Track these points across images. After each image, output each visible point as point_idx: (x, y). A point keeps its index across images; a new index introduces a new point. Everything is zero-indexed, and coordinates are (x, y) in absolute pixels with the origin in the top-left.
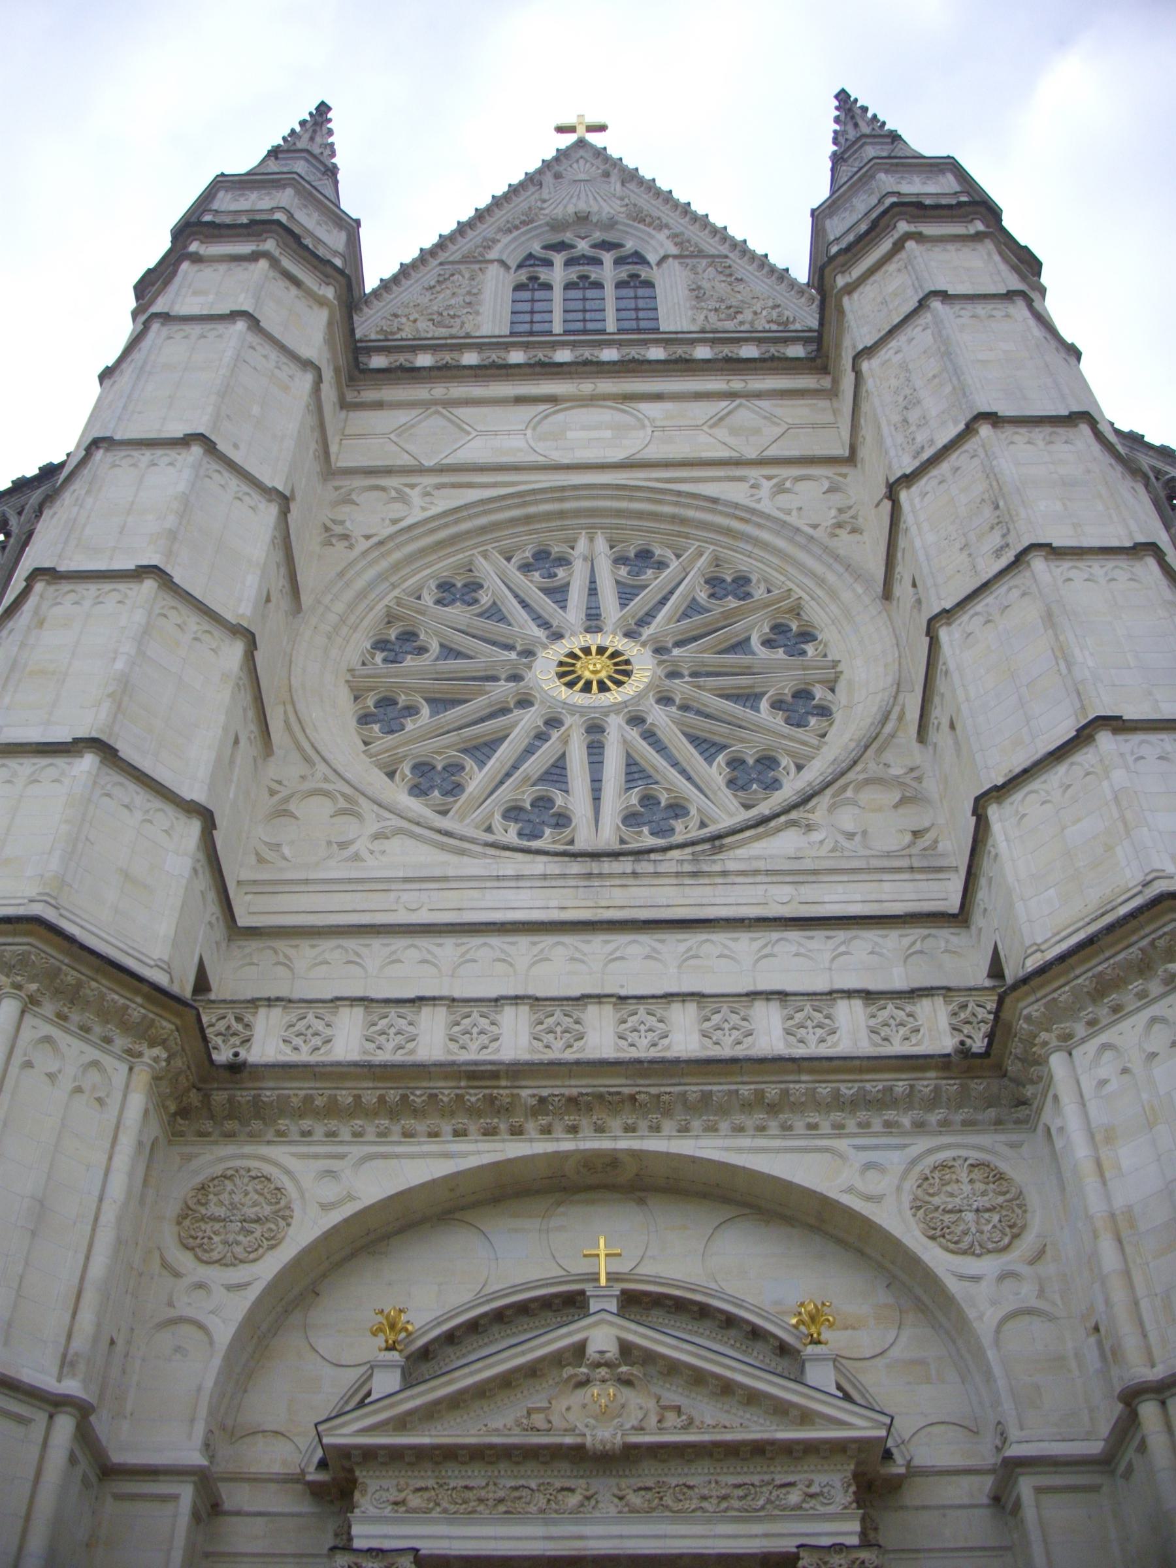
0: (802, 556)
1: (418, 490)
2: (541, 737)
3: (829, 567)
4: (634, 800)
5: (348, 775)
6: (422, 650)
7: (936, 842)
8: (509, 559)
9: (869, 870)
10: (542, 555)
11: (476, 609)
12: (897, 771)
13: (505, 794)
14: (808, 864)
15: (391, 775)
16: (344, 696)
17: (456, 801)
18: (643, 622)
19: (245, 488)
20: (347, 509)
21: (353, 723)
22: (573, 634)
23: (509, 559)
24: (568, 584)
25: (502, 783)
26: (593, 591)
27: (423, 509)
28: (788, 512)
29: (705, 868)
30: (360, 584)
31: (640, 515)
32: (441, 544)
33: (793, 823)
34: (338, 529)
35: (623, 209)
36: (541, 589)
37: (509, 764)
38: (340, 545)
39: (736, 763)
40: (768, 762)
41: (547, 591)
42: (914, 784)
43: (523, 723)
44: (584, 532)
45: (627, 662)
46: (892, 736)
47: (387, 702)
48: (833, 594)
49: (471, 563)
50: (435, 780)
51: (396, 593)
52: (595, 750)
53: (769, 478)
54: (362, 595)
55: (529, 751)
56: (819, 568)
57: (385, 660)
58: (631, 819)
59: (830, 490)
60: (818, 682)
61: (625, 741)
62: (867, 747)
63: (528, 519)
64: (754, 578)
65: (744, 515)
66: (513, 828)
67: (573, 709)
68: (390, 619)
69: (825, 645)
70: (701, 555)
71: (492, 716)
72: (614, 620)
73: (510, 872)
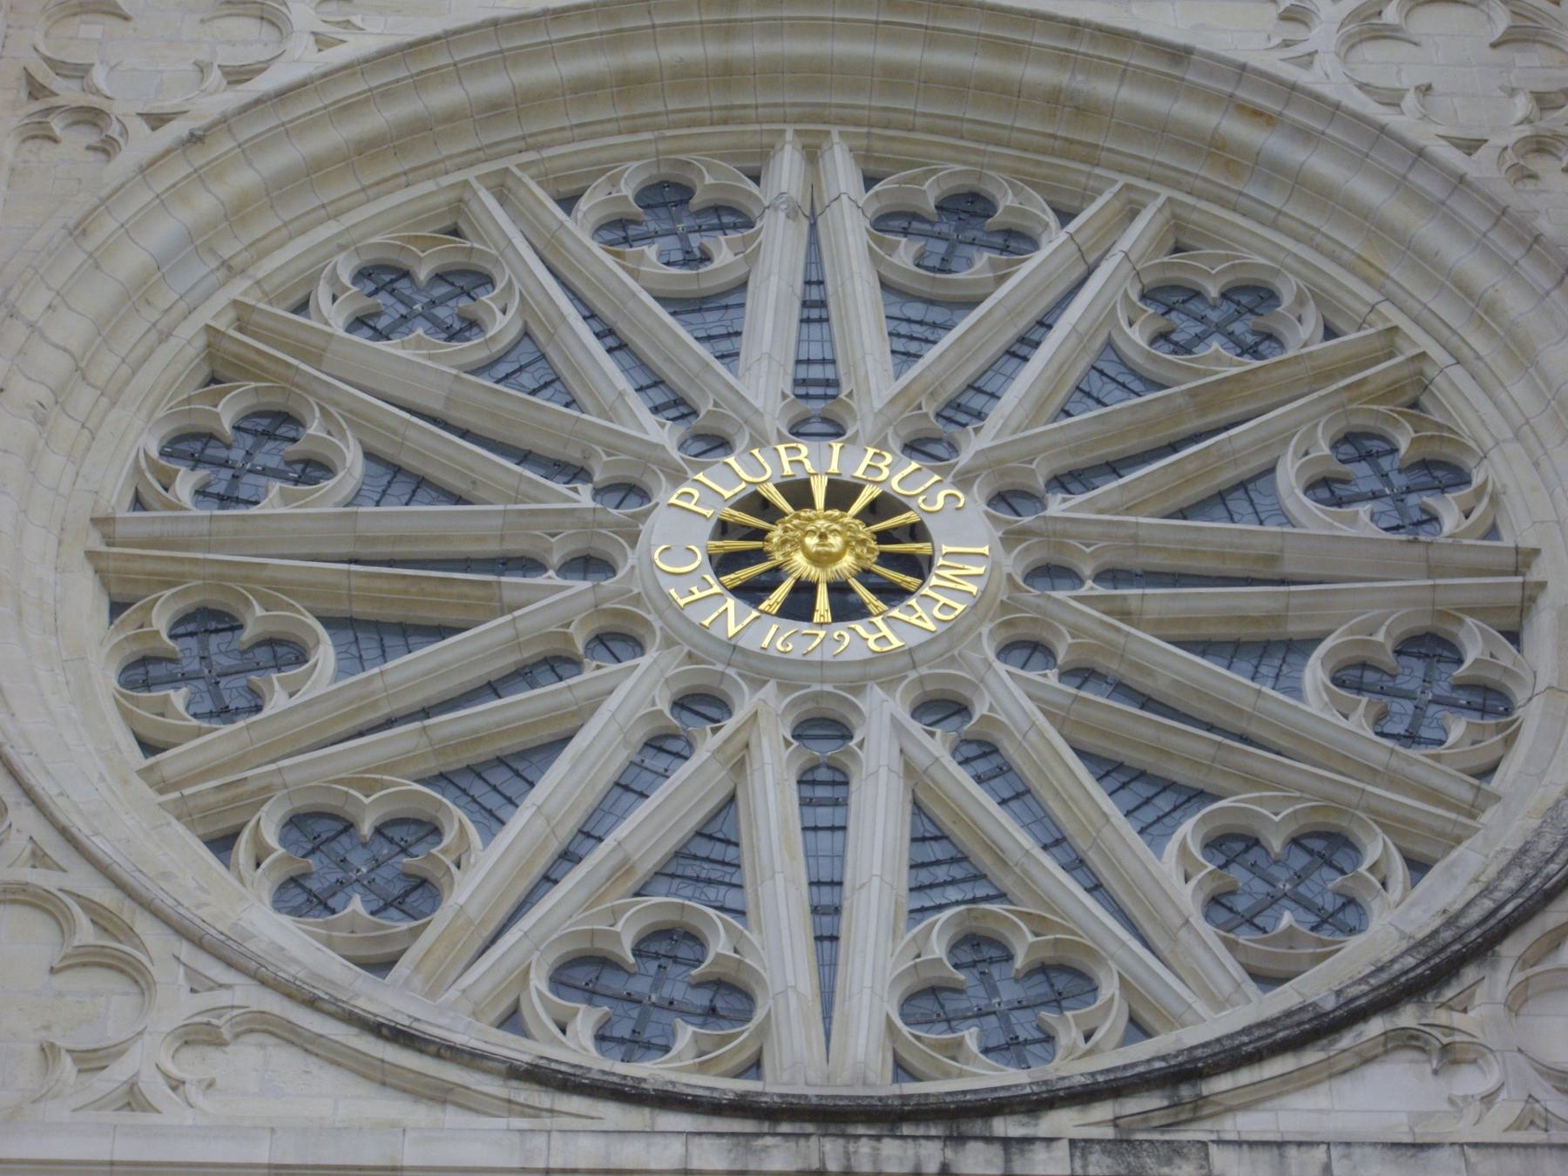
2: (663, 745)
3: (1510, 269)
4: (938, 949)
5: (101, 846)
6: (313, 469)
8: (568, 202)
10: (667, 195)
11: (472, 350)
13: (561, 914)
15: (222, 844)
16: (85, 598)
17: (415, 933)
18: (962, 409)
21: (106, 679)
22: (759, 441)
23: (568, 202)
25: (549, 880)
26: (815, 309)
27: (322, 42)
28: (1393, 100)
30: (131, 261)
31: (958, 86)
32: (368, 149)
33: (1408, 1040)
34: (68, 92)
36: (662, 300)
37: (572, 824)
38: (75, 141)
39: (1233, 844)
40: (1327, 844)
41: (681, 305)
43: (612, 703)
44: (790, 130)
45: (916, 532)
48: (1520, 352)
49: (458, 206)
50: (357, 864)
51: (238, 289)
52: (825, 787)
54: (138, 293)
55: (628, 788)
56: (1482, 274)
57: (201, 492)
58: (926, 1000)
60: (1472, 612)
61: (910, 769)
63: (629, 84)
66: (586, 1020)
67: (760, 668)
69: (1495, 501)
70: (1133, 214)
71: (524, 675)
72: (878, 405)
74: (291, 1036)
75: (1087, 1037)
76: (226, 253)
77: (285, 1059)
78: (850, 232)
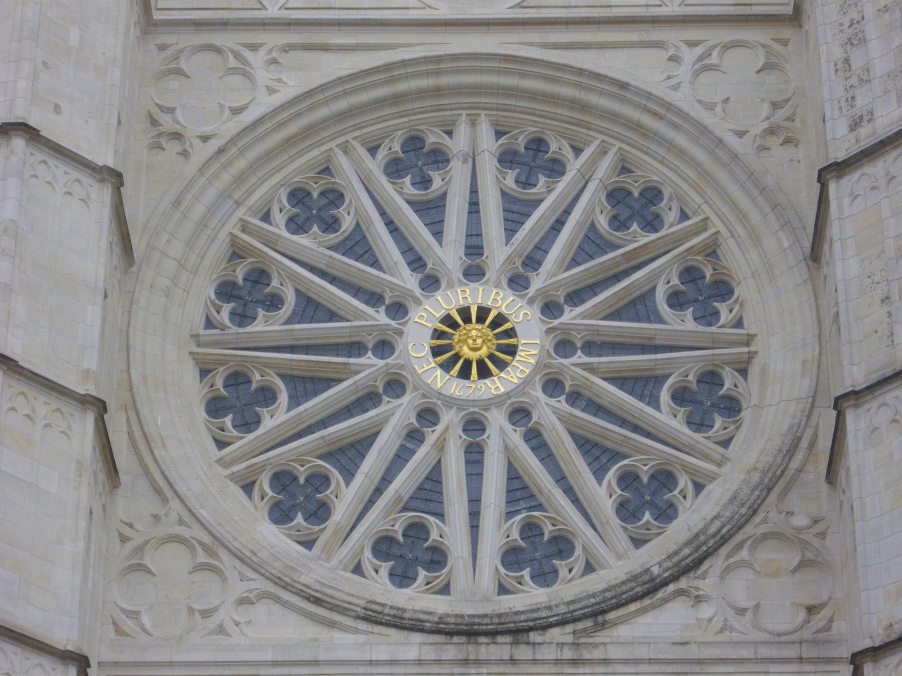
0: (722, 176)
1: (262, 52)
2: (414, 436)
3: (753, 200)
4: (515, 535)
5: (203, 513)
7: (831, 621)
8: (373, 151)
9: (757, 661)
12: (800, 521)
14: (693, 652)
15: (248, 488)
16: (190, 371)
17: (322, 530)
18: (533, 262)
19: (74, 174)
20: (174, 83)
22: (451, 285)
24: (444, 196)
26: (474, 207)
27: (271, 91)
29: (586, 655)
30: (199, 211)
31: (533, 95)
32: (291, 141)
33: (682, 592)
37: (379, 476)
38: (172, 147)
40: (664, 478)
41: (418, 207)
42: (816, 542)
43: (393, 422)
44: (464, 113)
45: (511, 333)
46: (800, 471)
47: (237, 379)
48: (757, 241)
49: (328, 159)
50: (297, 499)
51: (241, 213)
52: (474, 456)
53: (692, 44)
54: (203, 224)
55: (401, 457)
58: (512, 557)
59: (768, 67)
60: (727, 364)
61: (506, 448)
62: (769, 490)
63: (397, 99)
64: (667, 192)
65: (657, 109)
67: (450, 402)
68: (237, 253)
69: (741, 305)
70: (605, 153)
72: (498, 266)
73: (383, 657)
74: (278, 600)
75: (570, 571)
76: (236, 197)
77: (277, 609)
78: (488, 167)
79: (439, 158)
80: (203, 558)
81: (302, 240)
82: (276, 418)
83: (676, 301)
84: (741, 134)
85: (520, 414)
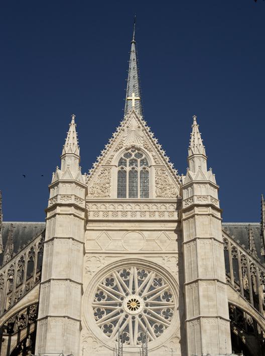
2: (125, 320)
8: (118, 272)
15: (100, 327)
26: (134, 282)
35: (142, 142)
38: (89, 273)
40: (161, 326)
50: (108, 329)
52: (133, 322)
54: (93, 286)
79: (128, 274)
80: (95, 340)
81: (108, 287)
82: (105, 316)
83: (163, 298)
84: (173, 272)
85: (140, 316)
